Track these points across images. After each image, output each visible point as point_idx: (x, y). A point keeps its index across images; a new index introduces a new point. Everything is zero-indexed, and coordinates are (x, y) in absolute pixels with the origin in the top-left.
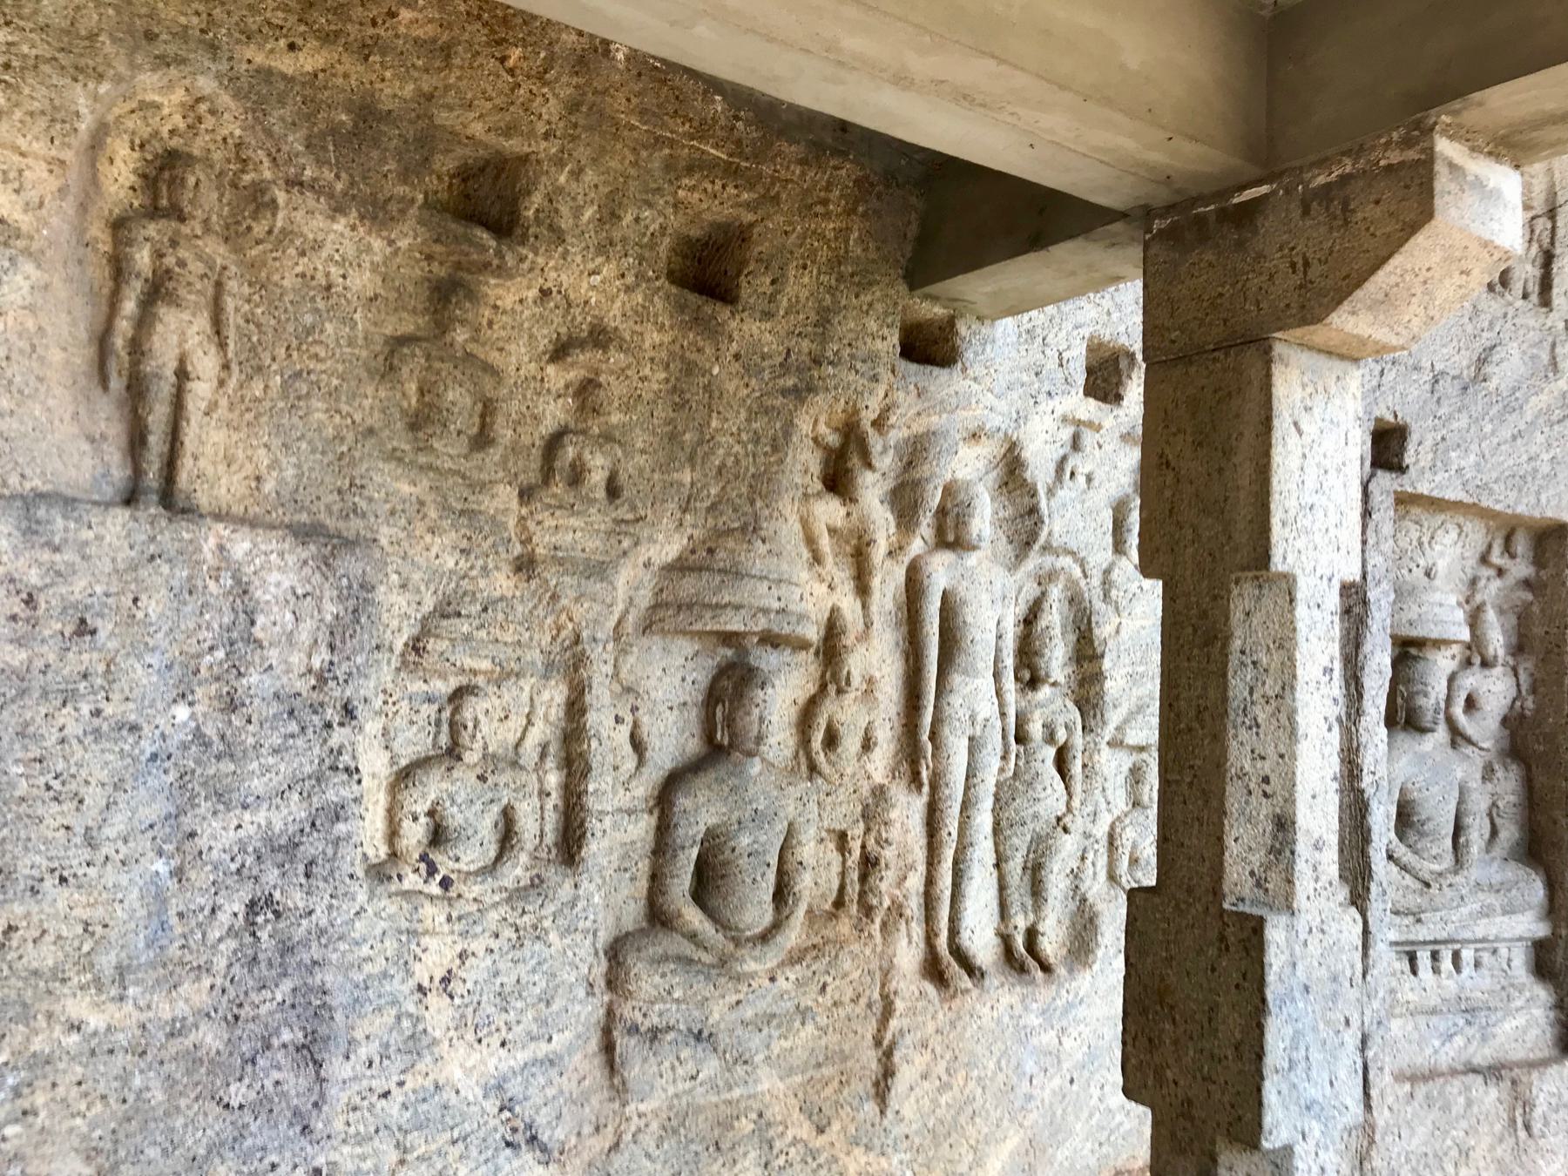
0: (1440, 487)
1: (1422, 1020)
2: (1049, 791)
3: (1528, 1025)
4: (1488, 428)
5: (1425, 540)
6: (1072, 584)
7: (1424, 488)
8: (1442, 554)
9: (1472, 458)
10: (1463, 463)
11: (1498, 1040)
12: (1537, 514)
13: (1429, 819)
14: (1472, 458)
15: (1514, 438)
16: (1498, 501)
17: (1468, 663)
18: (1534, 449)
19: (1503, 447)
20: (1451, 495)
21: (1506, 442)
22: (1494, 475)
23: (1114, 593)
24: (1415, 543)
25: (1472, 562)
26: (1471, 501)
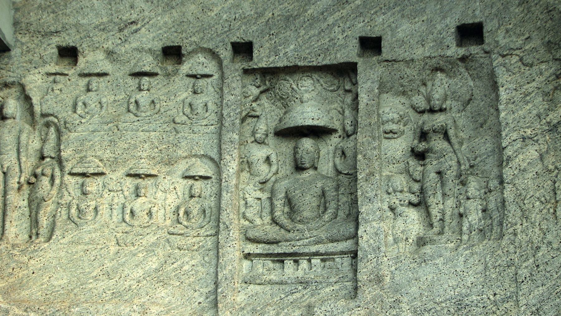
0: (273, 62)
1: (276, 287)
2: (41, 189)
3: (340, 289)
4: (303, 32)
5: (294, 86)
6: (55, 124)
7: (263, 65)
8: (306, 91)
9: (292, 47)
10: (287, 50)
11: (321, 296)
12: (335, 62)
13: (295, 205)
14: (292, 47)
15: (320, 33)
16: (310, 62)
17: (344, 138)
18: (332, 36)
19: (313, 38)
20: (280, 64)
21: (314, 35)
22: (308, 51)
23: (67, 125)
24: (291, 89)
25: (341, 92)
26: (291, 65)
